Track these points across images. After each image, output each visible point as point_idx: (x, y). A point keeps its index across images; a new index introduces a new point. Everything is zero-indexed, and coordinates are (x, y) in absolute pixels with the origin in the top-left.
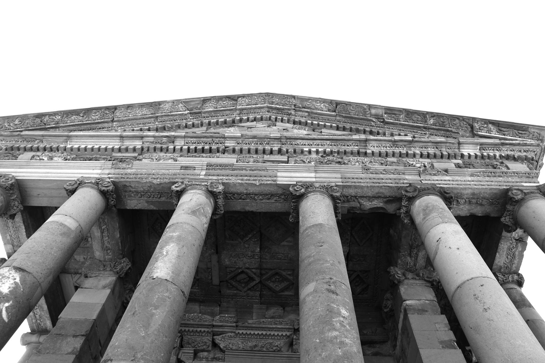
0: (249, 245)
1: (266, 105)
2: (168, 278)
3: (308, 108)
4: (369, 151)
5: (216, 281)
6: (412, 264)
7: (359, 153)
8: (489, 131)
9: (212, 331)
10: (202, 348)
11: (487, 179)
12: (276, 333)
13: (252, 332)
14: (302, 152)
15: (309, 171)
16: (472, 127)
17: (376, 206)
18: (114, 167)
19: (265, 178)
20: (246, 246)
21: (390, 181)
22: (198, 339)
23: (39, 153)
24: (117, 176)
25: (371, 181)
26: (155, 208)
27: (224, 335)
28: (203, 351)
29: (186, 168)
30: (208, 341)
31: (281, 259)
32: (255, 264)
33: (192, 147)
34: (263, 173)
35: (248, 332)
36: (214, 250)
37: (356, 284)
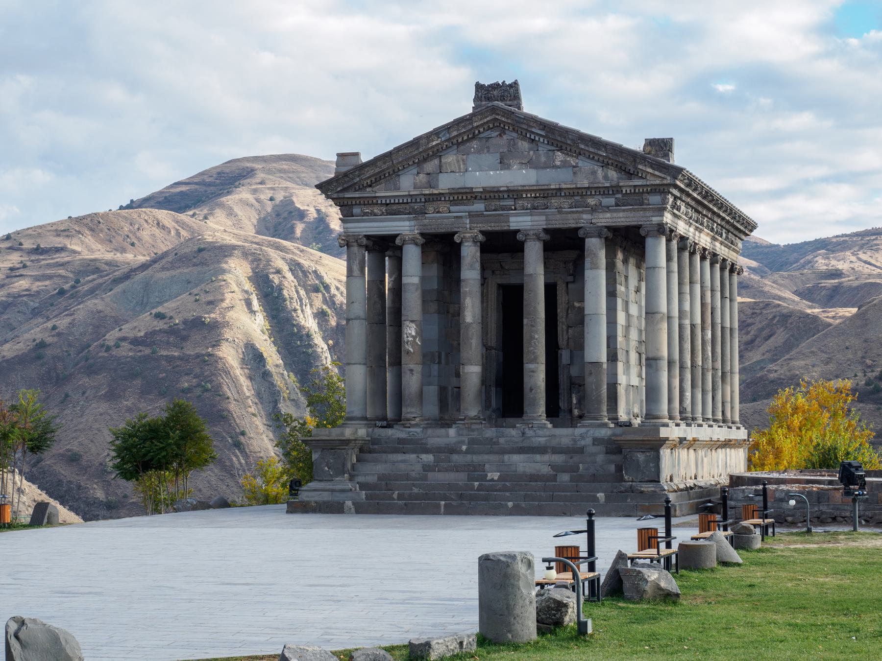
1: (494, 116)
4: (563, 194)
16: (635, 161)
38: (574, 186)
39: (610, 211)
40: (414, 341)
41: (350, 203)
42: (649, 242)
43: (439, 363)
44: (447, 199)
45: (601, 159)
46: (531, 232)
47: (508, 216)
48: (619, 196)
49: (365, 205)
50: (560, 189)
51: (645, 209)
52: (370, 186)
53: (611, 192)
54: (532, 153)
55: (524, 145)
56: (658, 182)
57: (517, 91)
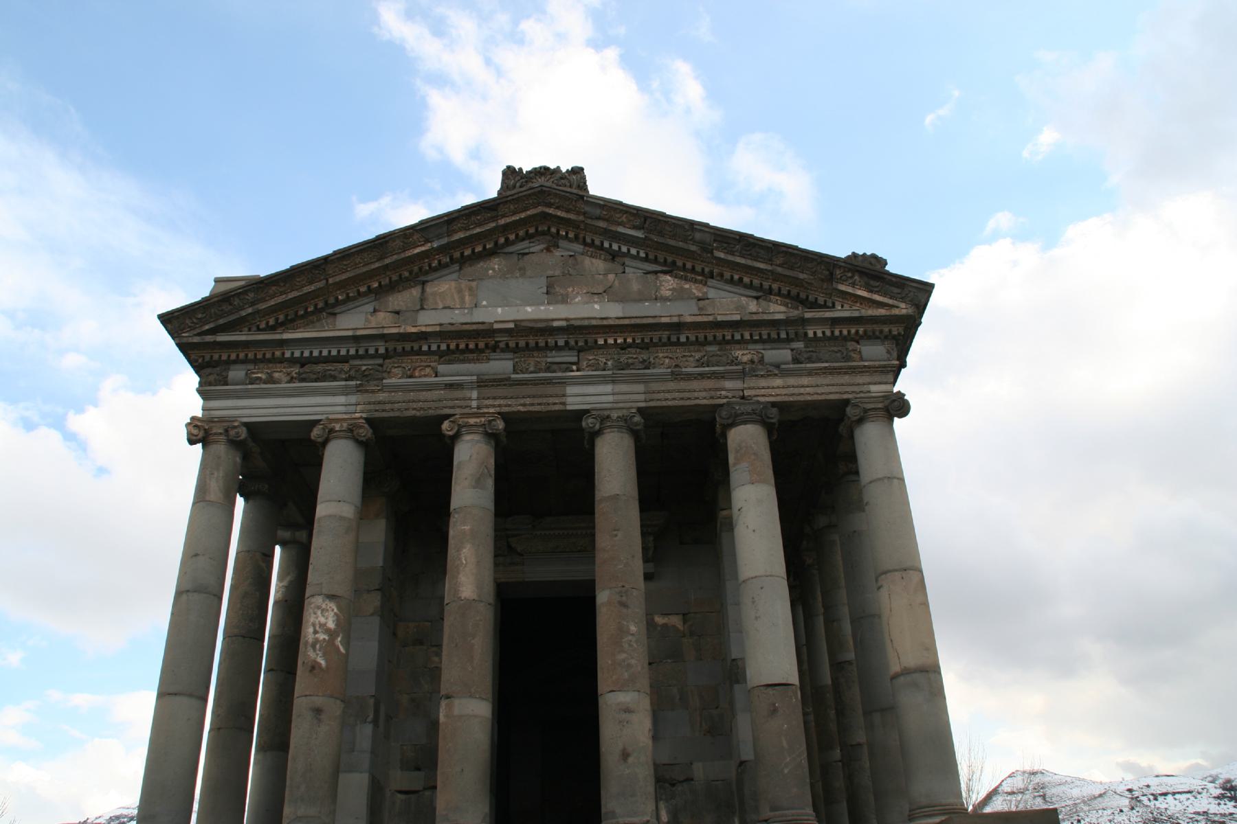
1: (540, 209)
2: (475, 597)
3: (604, 219)
4: (683, 339)
7: (670, 343)
8: (853, 285)
11: (829, 379)
14: (596, 342)
15: (604, 380)
16: (831, 274)
18: (359, 390)
19: (551, 400)
21: (704, 394)
23: (251, 366)
24: (369, 407)
25: (682, 395)
29: (450, 386)
33: (453, 346)
34: (550, 390)
38: (711, 318)
39: (785, 373)
40: (331, 641)
41: (224, 357)
42: (868, 435)
43: (375, 722)
44: (434, 348)
45: (756, 282)
46: (615, 415)
47: (563, 383)
48: (800, 345)
49: (255, 361)
50: (678, 327)
51: (853, 371)
52: (272, 329)
53: (783, 335)
54: (611, 277)
55: (596, 265)
56: (882, 312)
57: (584, 178)
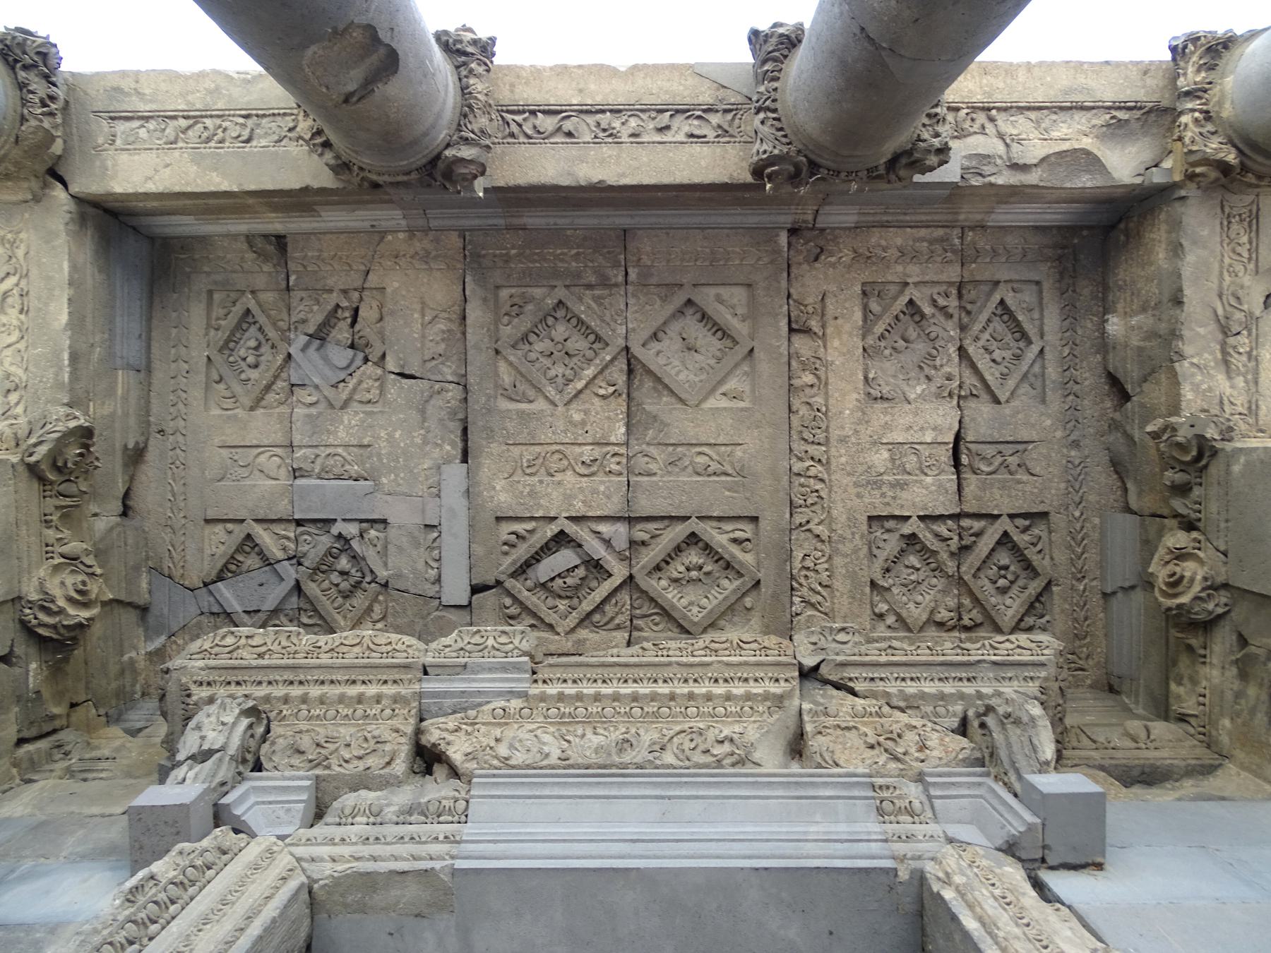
0: (586, 412)
5: (456, 589)
6: (1241, 402)
9: (421, 695)
10: (361, 765)
12: (720, 690)
13: (607, 690)
17: (1066, 146)
20: (577, 417)
22: (345, 732)
26: (225, 186)
27: (472, 713)
28: (361, 782)
30: (387, 735)
31: (705, 471)
32: (608, 497)
35: (588, 689)
36: (453, 444)
37: (1002, 582)
